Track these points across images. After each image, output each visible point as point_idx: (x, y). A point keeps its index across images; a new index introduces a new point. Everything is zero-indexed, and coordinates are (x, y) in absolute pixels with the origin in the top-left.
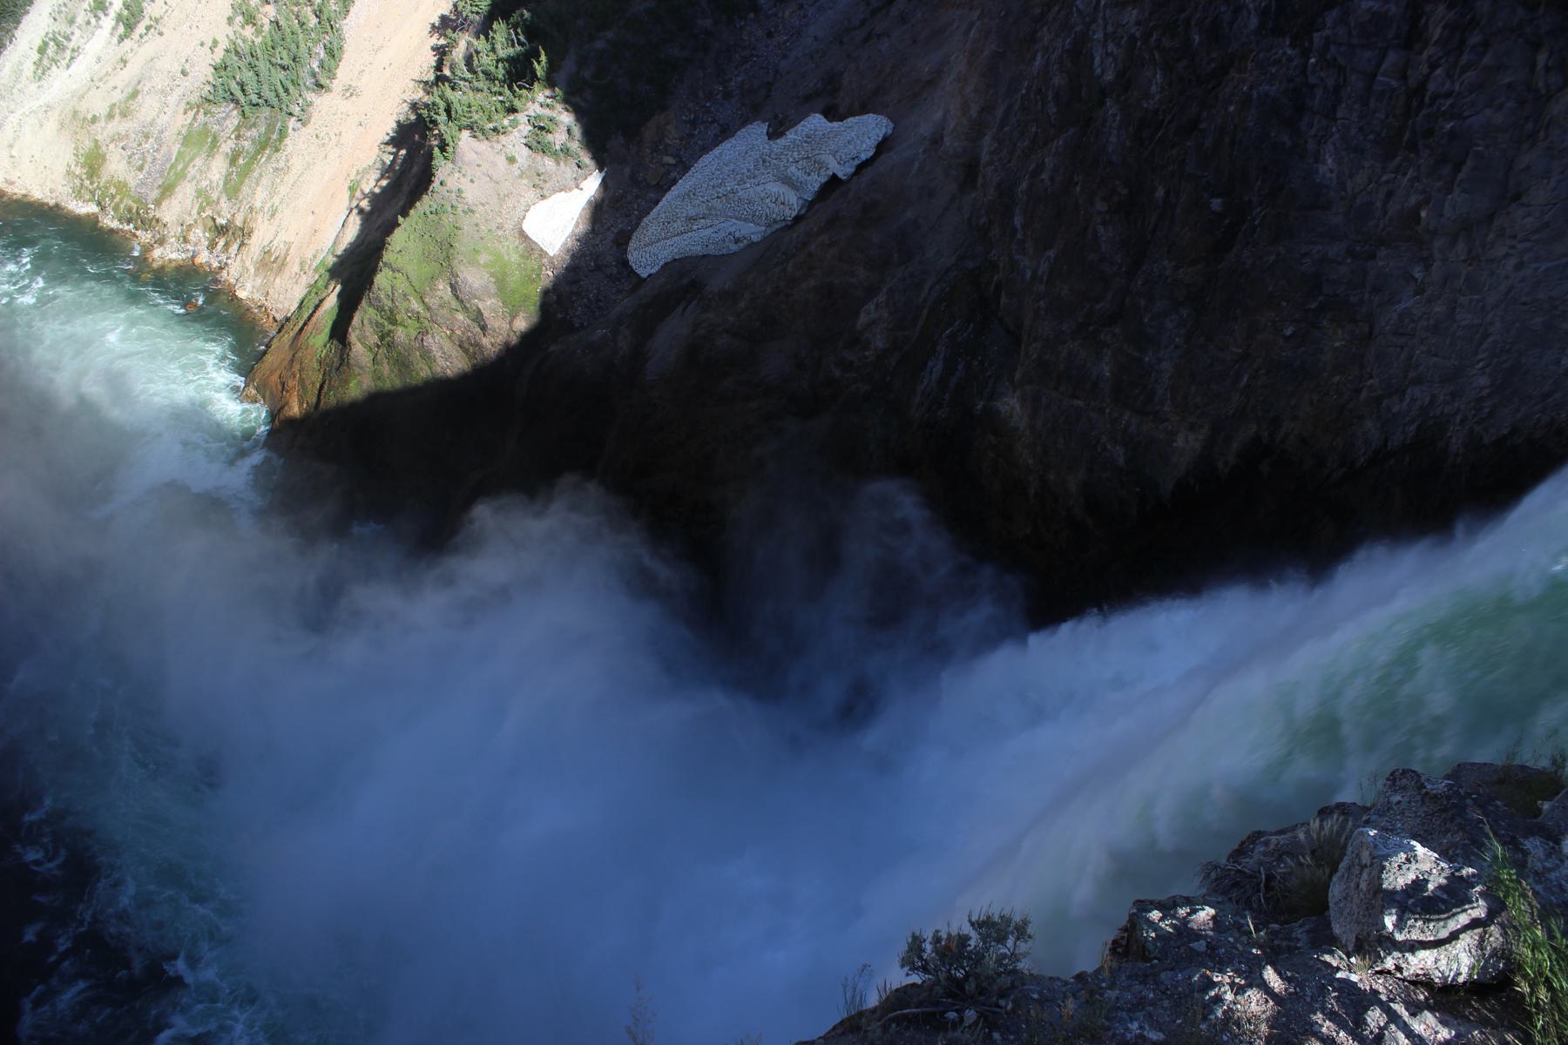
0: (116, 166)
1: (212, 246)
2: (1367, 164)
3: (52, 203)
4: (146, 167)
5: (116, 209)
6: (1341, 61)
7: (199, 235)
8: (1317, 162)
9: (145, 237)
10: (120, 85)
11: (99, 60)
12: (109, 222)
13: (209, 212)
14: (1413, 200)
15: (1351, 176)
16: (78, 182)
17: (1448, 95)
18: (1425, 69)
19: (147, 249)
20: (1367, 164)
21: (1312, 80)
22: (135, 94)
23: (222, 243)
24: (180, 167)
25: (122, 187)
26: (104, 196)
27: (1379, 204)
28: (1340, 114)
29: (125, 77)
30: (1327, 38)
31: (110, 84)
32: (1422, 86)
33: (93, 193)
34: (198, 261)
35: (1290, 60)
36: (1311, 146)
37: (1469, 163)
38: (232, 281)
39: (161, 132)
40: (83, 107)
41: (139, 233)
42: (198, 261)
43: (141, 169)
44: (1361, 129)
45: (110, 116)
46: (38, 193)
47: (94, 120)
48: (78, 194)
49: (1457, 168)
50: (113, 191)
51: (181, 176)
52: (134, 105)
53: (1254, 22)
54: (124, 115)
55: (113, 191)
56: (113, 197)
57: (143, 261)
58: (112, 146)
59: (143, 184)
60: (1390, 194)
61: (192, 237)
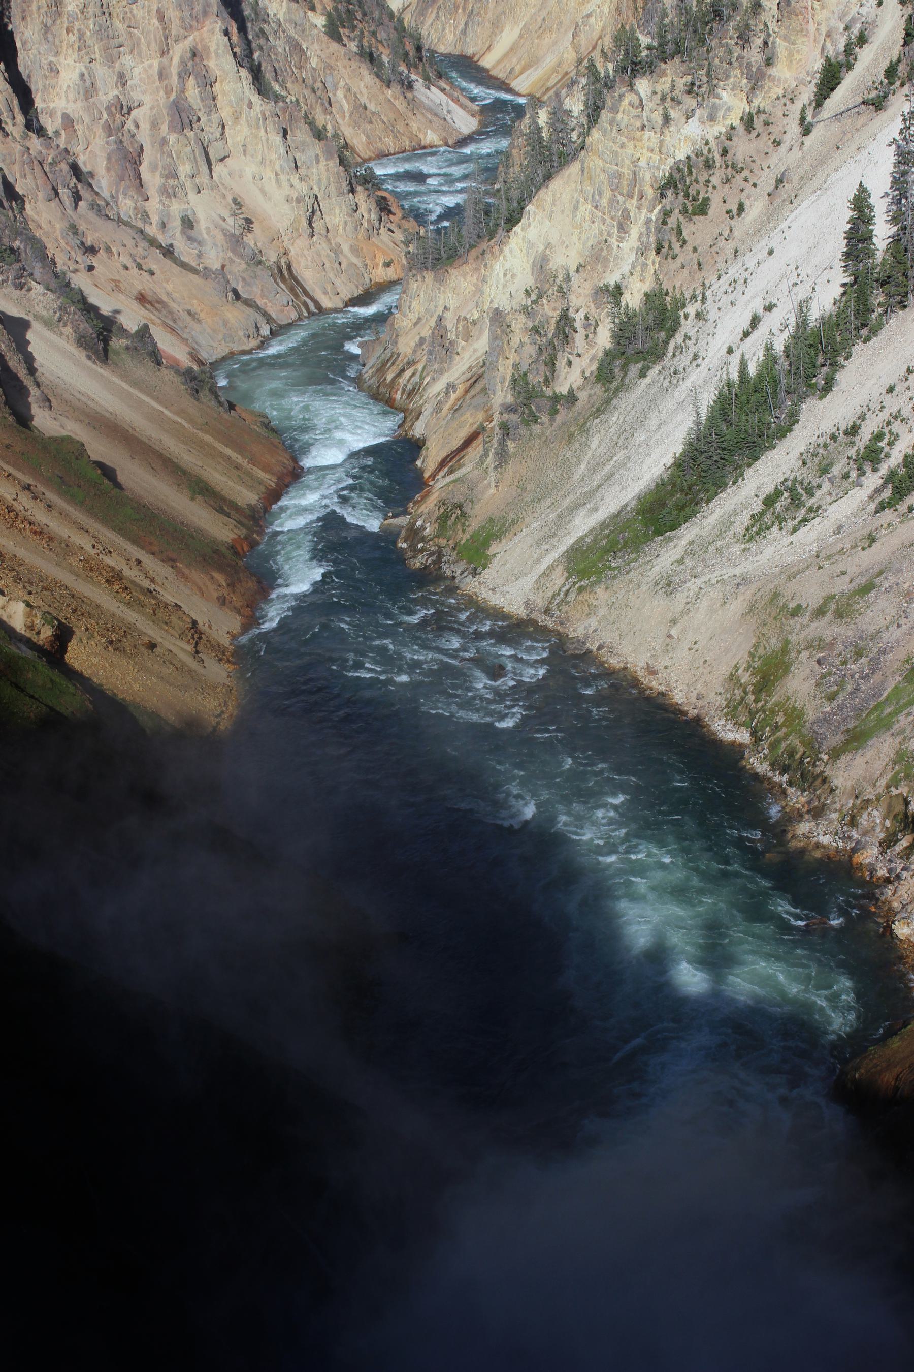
0: (799, 685)
1: (888, 843)
3: (693, 713)
4: (841, 697)
5: (773, 747)
7: (875, 820)
9: (797, 798)
10: (852, 570)
11: (839, 529)
12: (758, 764)
13: (903, 790)
16: (738, 693)
19: (791, 817)
22: (866, 589)
23: (905, 843)
24: (888, 710)
25: (795, 716)
26: (764, 723)
29: (865, 560)
31: (841, 566)
33: (752, 714)
34: (859, 858)
38: (896, 905)
39: (882, 652)
40: (789, 589)
41: (791, 790)
42: (859, 858)
43: (831, 698)
45: (820, 612)
46: (678, 697)
47: (797, 612)
48: (732, 712)
50: (780, 719)
51: (885, 724)
52: (859, 604)
54: (839, 615)
55: (780, 719)
56: (776, 727)
57: (777, 832)
58: (805, 654)
59: (825, 720)
61: (864, 820)
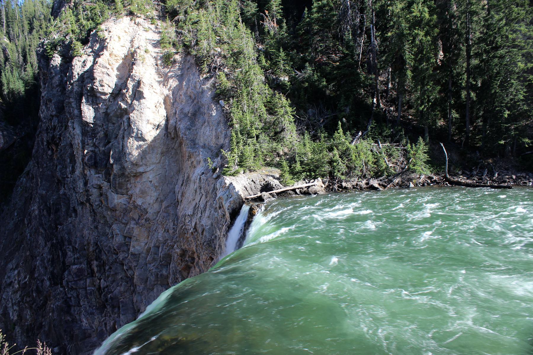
2: (96, 317)
6: (74, 287)
8: (81, 322)
14: (112, 324)
15: (93, 323)
17: (107, 287)
18: (98, 281)
20: (96, 317)
21: (69, 296)
27: (104, 329)
28: (82, 304)
30: (67, 281)
32: (100, 285)
35: (61, 292)
36: (78, 317)
37: (121, 306)
44: (90, 306)
49: (119, 307)
53: (48, 283)
60: (106, 324)
